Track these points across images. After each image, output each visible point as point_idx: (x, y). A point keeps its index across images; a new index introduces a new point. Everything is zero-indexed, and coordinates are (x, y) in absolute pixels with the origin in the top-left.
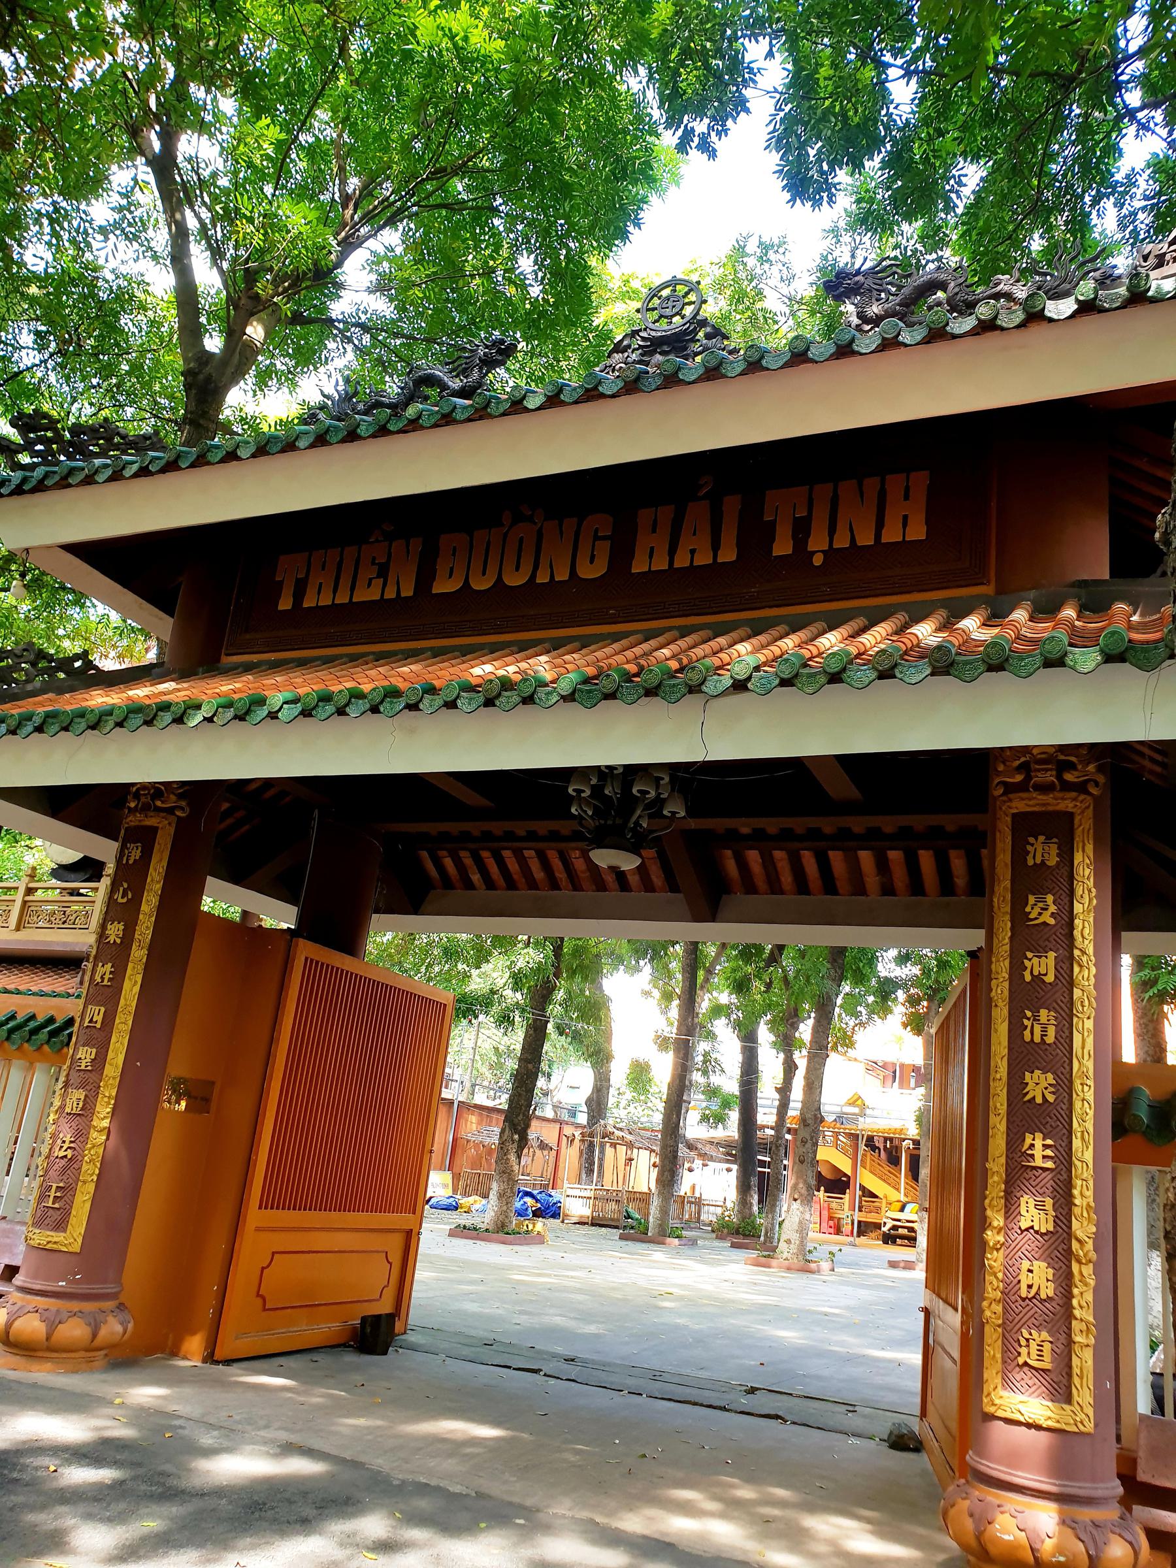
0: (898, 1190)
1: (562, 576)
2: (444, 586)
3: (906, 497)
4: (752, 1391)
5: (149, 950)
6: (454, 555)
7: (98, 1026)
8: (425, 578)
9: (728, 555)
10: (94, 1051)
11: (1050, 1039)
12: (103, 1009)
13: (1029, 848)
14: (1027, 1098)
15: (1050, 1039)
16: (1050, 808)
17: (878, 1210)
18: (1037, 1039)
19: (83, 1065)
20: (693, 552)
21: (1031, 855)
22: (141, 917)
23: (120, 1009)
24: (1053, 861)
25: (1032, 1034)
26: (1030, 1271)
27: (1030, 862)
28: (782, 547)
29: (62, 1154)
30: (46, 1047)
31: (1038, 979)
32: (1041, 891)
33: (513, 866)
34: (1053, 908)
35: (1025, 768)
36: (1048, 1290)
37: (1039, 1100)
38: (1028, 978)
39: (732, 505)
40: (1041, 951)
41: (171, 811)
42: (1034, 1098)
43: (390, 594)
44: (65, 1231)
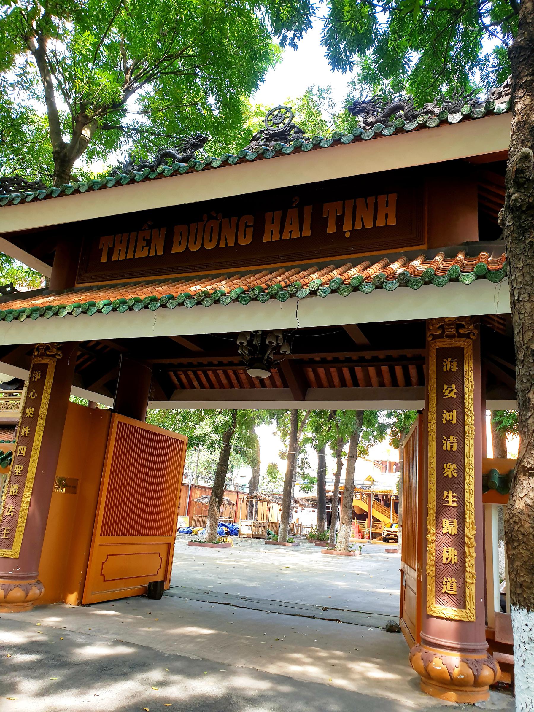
0: (389, 518)
1: (231, 244)
2: (177, 250)
3: (387, 206)
4: (326, 609)
5: (46, 420)
6: (181, 235)
7: (24, 455)
8: (168, 246)
9: (307, 233)
10: (22, 467)
11: (455, 449)
12: (25, 448)
13: (444, 363)
14: (445, 475)
15: (455, 449)
16: (454, 346)
17: (380, 527)
18: (449, 449)
20: (291, 232)
21: (445, 367)
22: (42, 405)
23: (33, 447)
24: (455, 369)
25: (447, 447)
26: (447, 552)
27: (445, 370)
28: (331, 229)
29: (9, 514)
31: (449, 422)
32: (449, 383)
33: (212, 378)
34: (455, 390)
35: (442, 327)
36: (455, 560)
37: (450, 476)
38: (444, 422)
39: (308, 210)
40: (450, 410)
41: (54, 356)
42: (448, 475)
43: (152, 254)
44: (11, 549)
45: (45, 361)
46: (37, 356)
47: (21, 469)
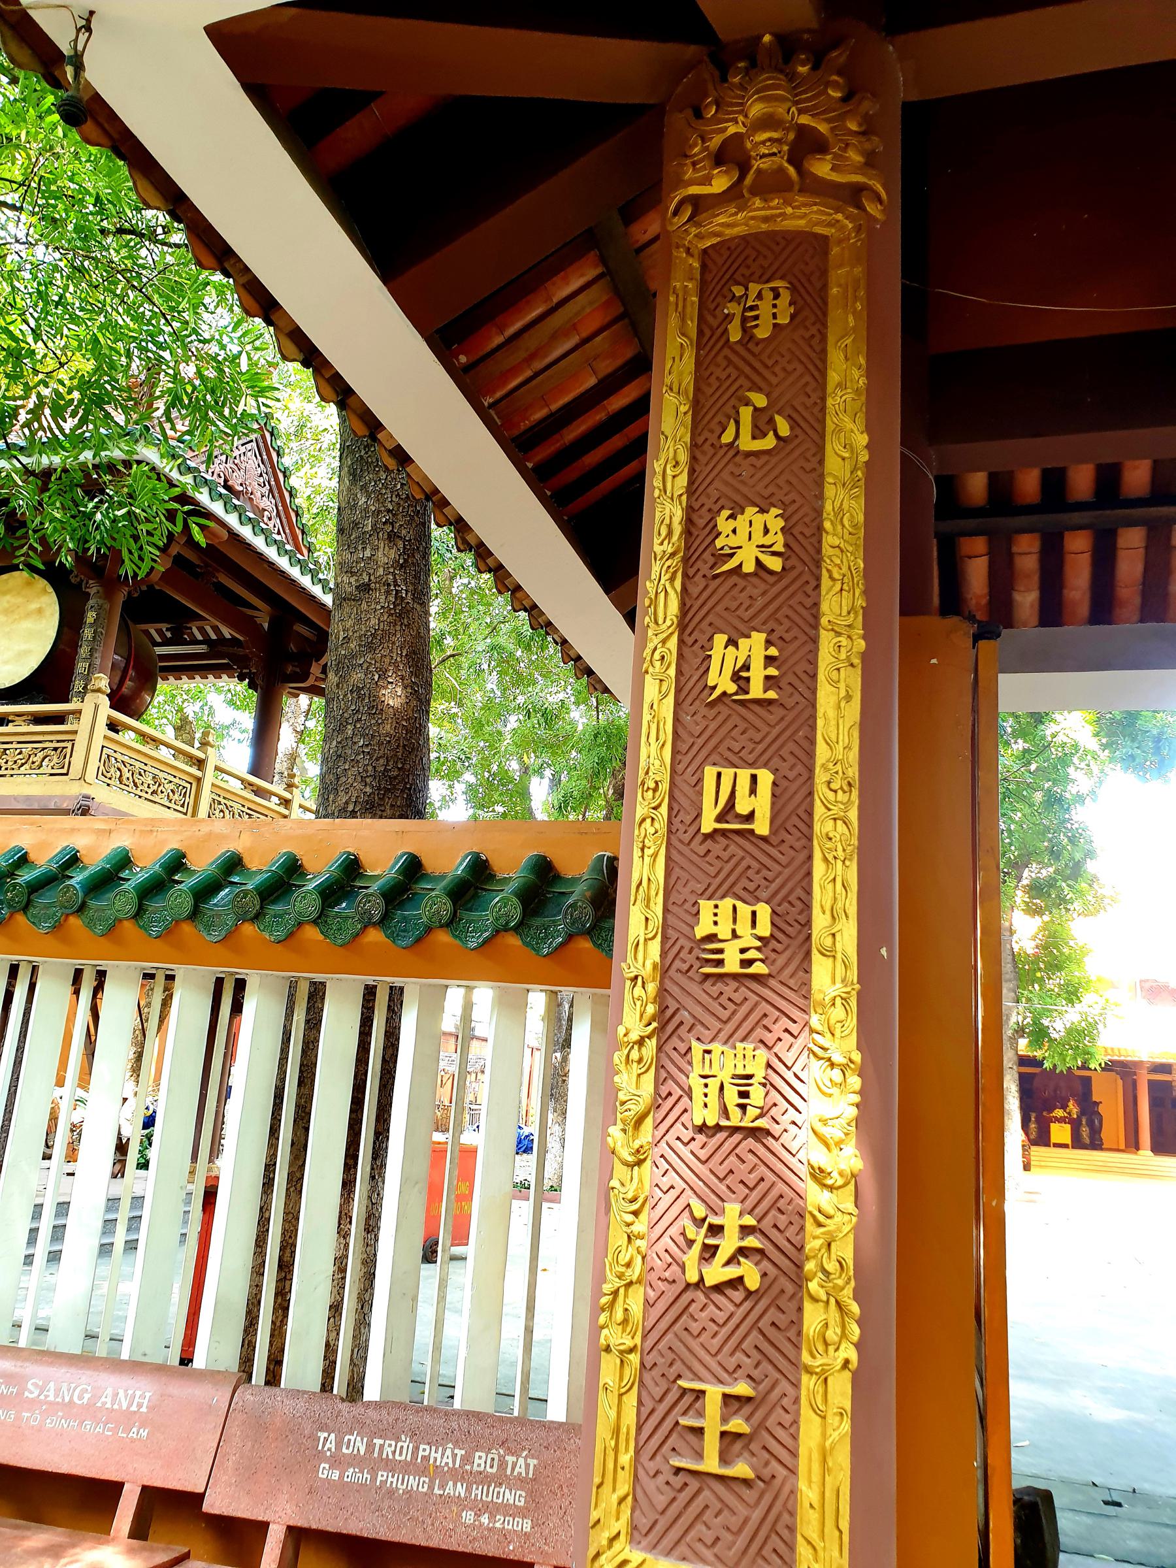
7: (762, 827)
10: (764, 911)
12: (766, 778)
19: (732, 964)
22: (829, 491)
23: (820, 777)
29: (716, 1273)
30: (312, 933)
41: (854, 195)
45: (801, 216)
46: (732, 195)
47: (764, 929)
